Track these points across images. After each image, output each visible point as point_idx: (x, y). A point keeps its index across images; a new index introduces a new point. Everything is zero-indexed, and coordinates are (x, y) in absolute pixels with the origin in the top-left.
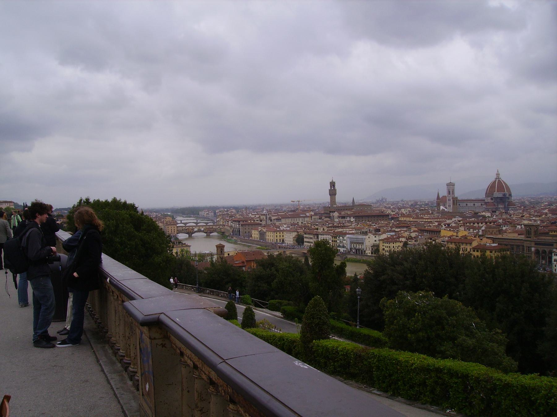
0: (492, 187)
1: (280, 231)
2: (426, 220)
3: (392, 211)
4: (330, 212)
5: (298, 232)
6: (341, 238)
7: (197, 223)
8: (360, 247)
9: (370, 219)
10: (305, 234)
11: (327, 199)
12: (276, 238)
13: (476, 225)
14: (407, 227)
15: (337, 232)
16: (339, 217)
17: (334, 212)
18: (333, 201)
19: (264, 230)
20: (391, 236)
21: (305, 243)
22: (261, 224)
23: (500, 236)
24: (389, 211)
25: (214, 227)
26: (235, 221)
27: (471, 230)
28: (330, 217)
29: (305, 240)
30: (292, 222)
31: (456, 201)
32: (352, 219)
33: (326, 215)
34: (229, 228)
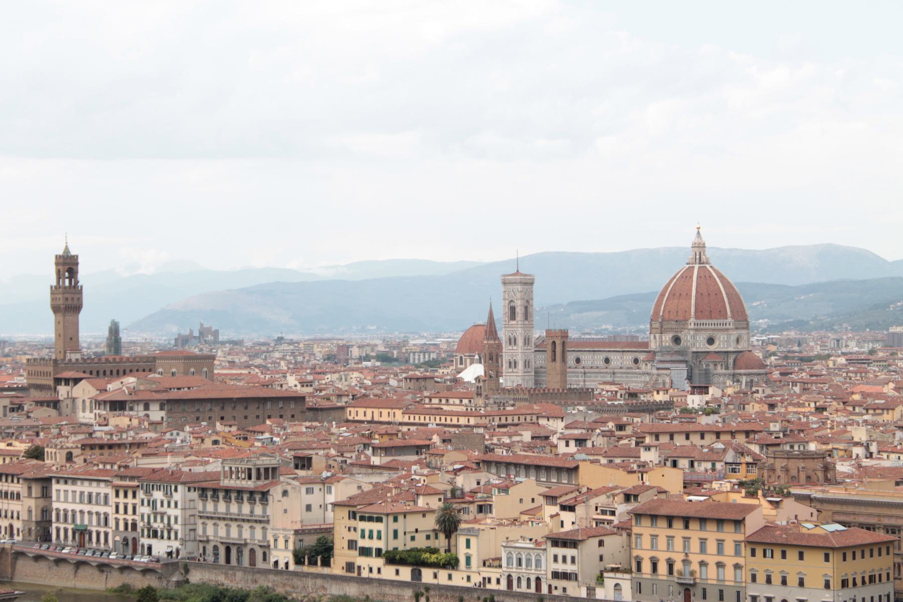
0: (677, 290)
2: (463, 421)
3: (303, 383)
4: (58, 381)
8: (246, 534)
9: (228, 411)
11: (43, 328)
13: (680, 440)
14: (418, 449)
15: (137, 469)
16: (99, 403)
17: (77, 381)
18: (68, 336)
20: (376, 485)
23: (834, 492)
24: (292, 381)
27: (684, 463)
28: (55, 404)
31: (558, 346)
32: (156, 414)
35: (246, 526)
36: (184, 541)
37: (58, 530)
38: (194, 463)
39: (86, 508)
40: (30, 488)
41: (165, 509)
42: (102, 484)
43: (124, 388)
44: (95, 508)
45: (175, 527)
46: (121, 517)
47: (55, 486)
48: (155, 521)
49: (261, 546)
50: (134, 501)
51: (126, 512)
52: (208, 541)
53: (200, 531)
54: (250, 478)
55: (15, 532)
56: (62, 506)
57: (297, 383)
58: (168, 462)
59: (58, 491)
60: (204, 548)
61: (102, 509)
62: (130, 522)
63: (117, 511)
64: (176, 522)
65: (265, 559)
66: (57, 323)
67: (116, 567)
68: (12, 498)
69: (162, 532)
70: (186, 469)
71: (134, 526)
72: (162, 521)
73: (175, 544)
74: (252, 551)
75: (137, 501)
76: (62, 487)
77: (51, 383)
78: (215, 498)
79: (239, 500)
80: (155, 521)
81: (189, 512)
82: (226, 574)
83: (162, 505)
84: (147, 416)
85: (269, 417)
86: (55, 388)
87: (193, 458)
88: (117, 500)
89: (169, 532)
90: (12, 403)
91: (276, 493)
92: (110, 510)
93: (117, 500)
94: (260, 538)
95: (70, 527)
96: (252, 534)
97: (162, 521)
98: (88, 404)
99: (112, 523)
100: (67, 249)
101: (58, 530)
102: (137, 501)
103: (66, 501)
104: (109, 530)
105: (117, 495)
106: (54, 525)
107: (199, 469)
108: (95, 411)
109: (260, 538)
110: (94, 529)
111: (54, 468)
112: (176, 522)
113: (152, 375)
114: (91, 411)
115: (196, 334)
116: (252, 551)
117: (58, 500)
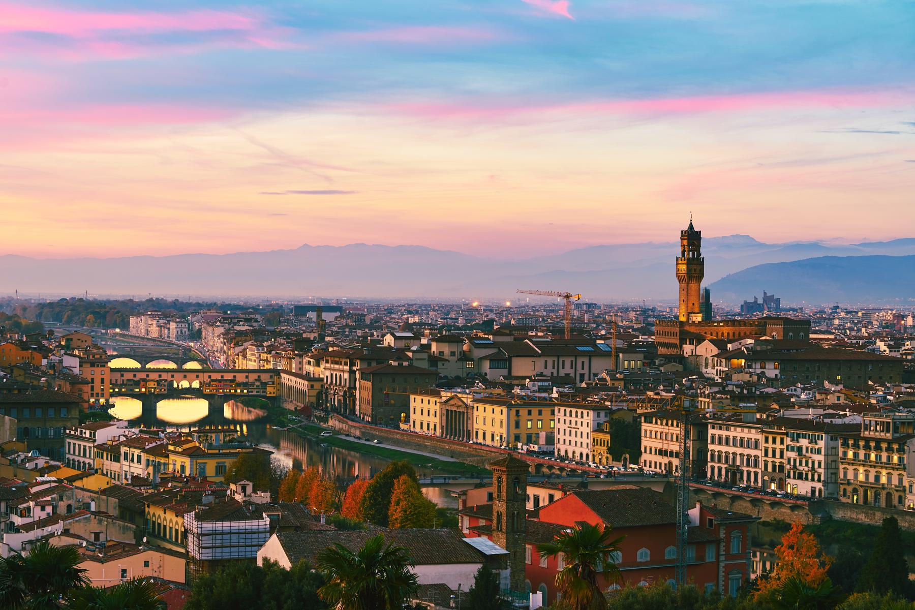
1: (529, 403)
4: (683, 341)
5: (610, 412)
7: (144, 358)
10: (648, 418)
12: (514, 431)
19: (468, 400)
21: (645, 457)
22: (437, 374)
25: (241, 378)
26: (336, 358)
28: (681, 359)
29: (645, 442)
30: (547, 372)
32: (772, 371)
33: (661, 350)
34: (302, 384)
35: (884, 472)
36: (825, 483)
37: (713, 468)
38: (833, 416)
39: (739, 451)
41: (809, 454)
42: (753, 431)
43: (743, 348)
44: (746, 452)
45: (820, 470)
46: (770, 460)
47: (711, 431)
48: (801, 464)
49: (897, 491)
50: (782, 447)
51: (774, 456)
52: (849, 483)
53: (841, 475)
54: (888, 431)
55: (674, 469)
57: (885, 348)
58: (811, 413)
60: (845, 490)
61: (753, 452)
62: (778, 464)
63: (766, 455)
64: (820, 466)
65: (901, 500)
66: (682, 290)
67: (768, 502)
69: (807, 474)
70: (827, 420)
71: (782, 468)
72: (807, 465)
73: (819, 486)
74: (889, 495)
76: (717, 432)
77: (678, 342)
79: (878, 448)
80: (801, 464)
81: (831, 458)
82: (866, 513)
83: (807, 451)
84: (763, 373)
85: (870, 378)
86: (681, 347)
87: (831, 411)
88: (766, 445)
89: (813, 476)
90: (645, 358)
93: (766, 445)
94: (897, 484)
95: (724, 466)
96: (889, 480)
97: (807, 465)
98: (710, 361)
99: (762, 465)
100: (691, 226)
101: (713, 468)
102: (784, 447)
104: (759, 471)
105: (767, 441)
106: (709, 464)
107: (838, 421)
109: (897, 484)
110: (745, 469)
111: (708, 415)
112: (820, 466)
113: (763, 338)
114: (713, 367)
115: (760, 301)
116: (889, 495)
117: (713, 442)
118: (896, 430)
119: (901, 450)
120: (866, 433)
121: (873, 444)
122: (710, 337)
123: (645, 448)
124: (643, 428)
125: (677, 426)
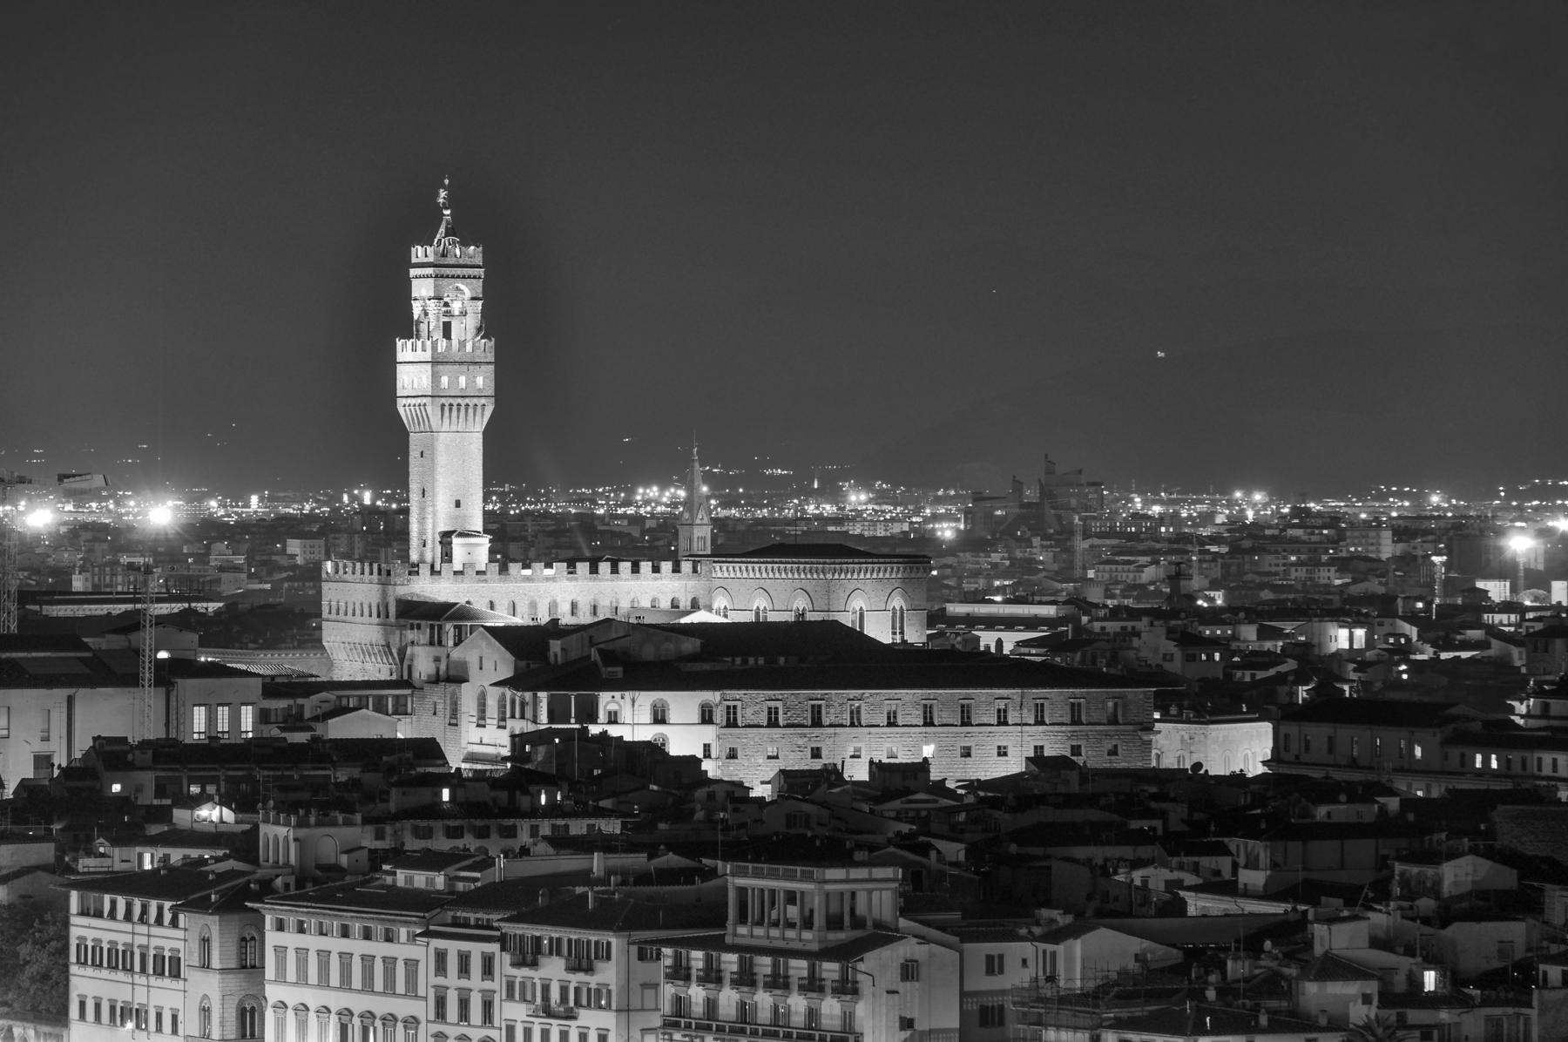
6: (553, 970)
29: (85, 983)
40: (205, 942)
43: (594, 655)
47: (272, 938)
50: (488, 985)
51: (464, 1015)
54: (808, 923)
56: (292, 996)
57: (1170, 647)
59: (281, 951)
61: (403, 1008)
63: (441, 1014)
68: (159, 973)
75: (495, 985)
76: (290, 939)
78: (712, 976)
87: (671, 859)
91: (879, 964)
92: (421, 1009)
93: (441, 981)
103: (302, 980)
105: (441, 968)
108: (510, 723)
117: (281, 978)
118: (834, 923)
119: (847, 988)
120: (742, 930)
121: (764, 964)
122: (501, 619)
123: (82, 1005)
124: (75, 933)
125: (174, 923)
